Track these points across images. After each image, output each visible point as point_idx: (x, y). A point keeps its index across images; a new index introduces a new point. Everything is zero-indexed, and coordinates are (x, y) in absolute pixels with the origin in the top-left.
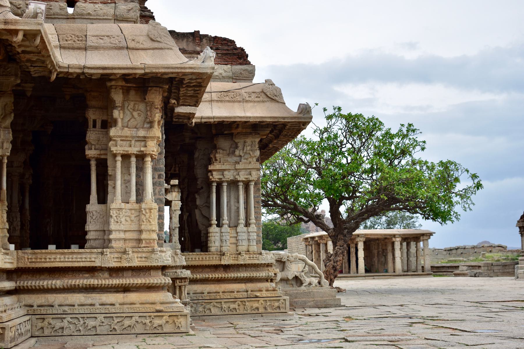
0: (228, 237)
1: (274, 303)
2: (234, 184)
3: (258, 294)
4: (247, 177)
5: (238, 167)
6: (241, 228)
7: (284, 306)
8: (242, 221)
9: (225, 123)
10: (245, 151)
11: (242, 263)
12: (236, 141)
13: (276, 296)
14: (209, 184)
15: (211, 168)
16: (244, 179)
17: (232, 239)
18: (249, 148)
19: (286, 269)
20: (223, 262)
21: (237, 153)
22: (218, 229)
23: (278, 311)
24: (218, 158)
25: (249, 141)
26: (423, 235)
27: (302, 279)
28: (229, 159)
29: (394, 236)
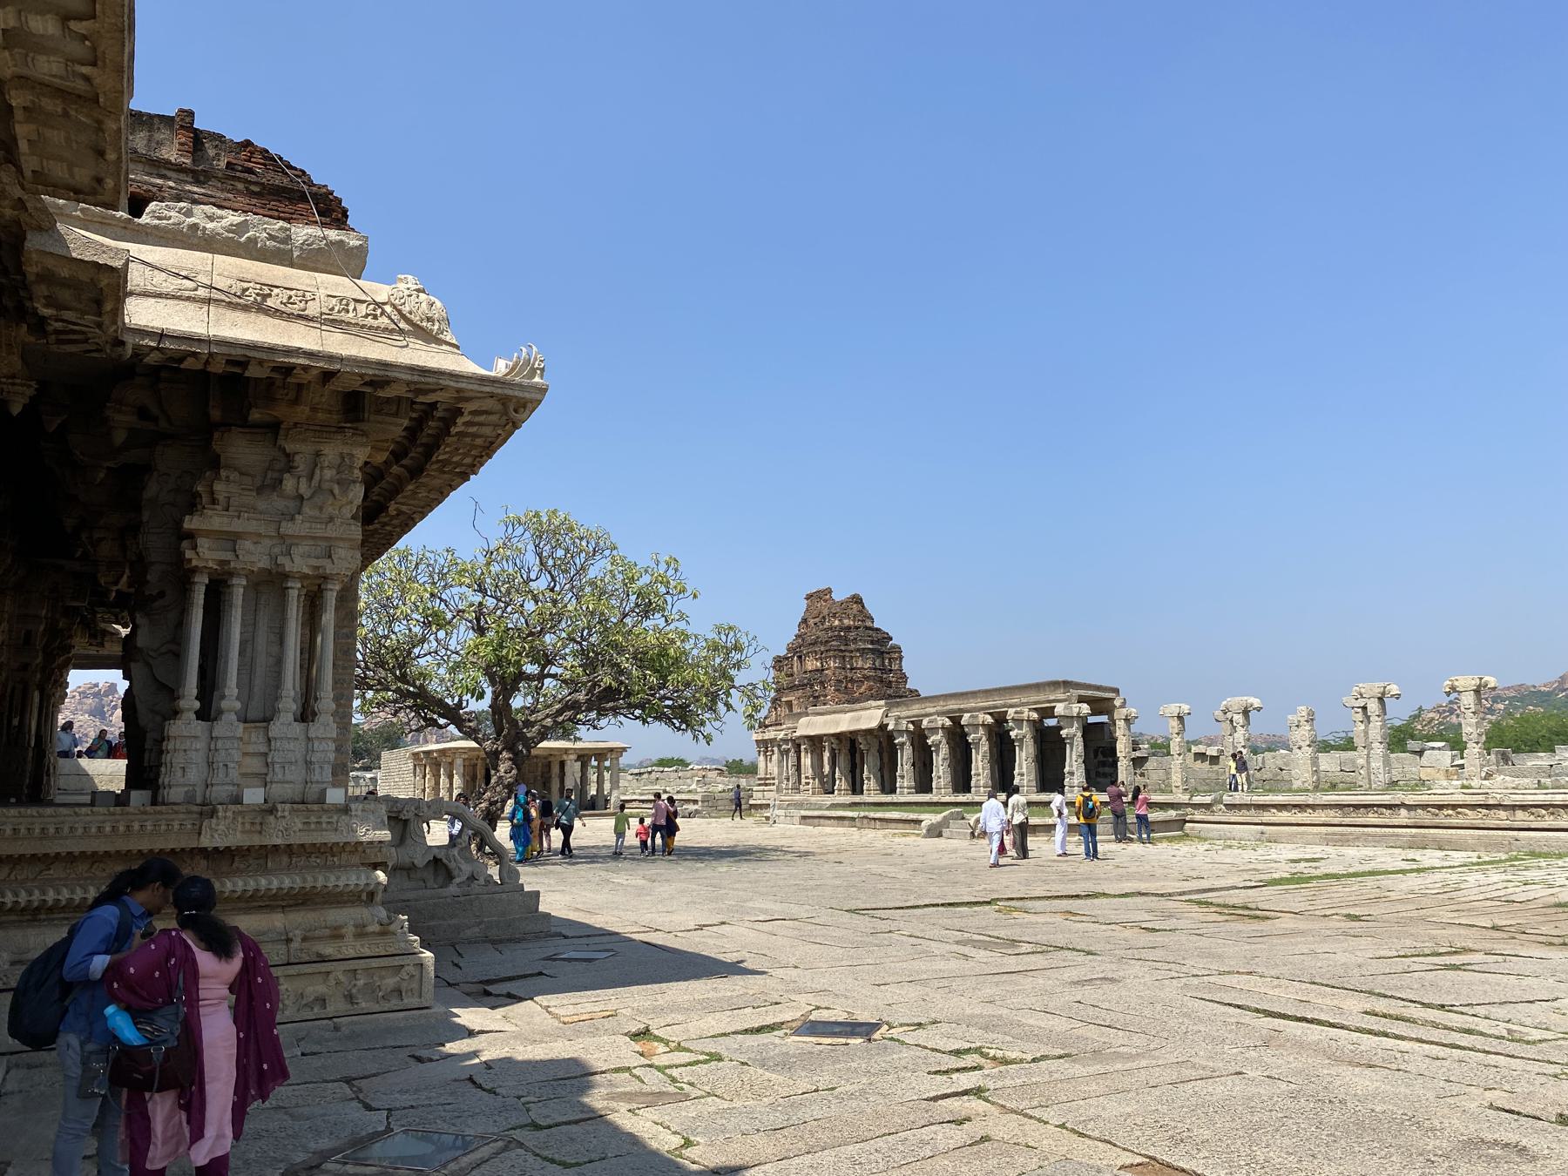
0: (236, 756)
1: (382, 978)
2: (272, 582)
3: (328, 950)
4: (314, 562)
5: (288, 528)
6: (285, 725)
7: (415, 985)
8: (289, 703)
9: (253, 372)
10: (315, 482)
11: (279, 842)
12: (290, 447)
13: (391, 951)
14: (183, 577)
15: (190, 523)
16: (306, 570)
17: (248, 760)
18: (328, 474)
19: (409, 841)
20: (206, 842)
21: (289, 484)
22: (199, 727)
23: (394, 1003)
24: (221, 498)
25: (331, 451)
26: (612, 750)
27: (452, 865)
28: (261, 504)
29: (566, 751)
